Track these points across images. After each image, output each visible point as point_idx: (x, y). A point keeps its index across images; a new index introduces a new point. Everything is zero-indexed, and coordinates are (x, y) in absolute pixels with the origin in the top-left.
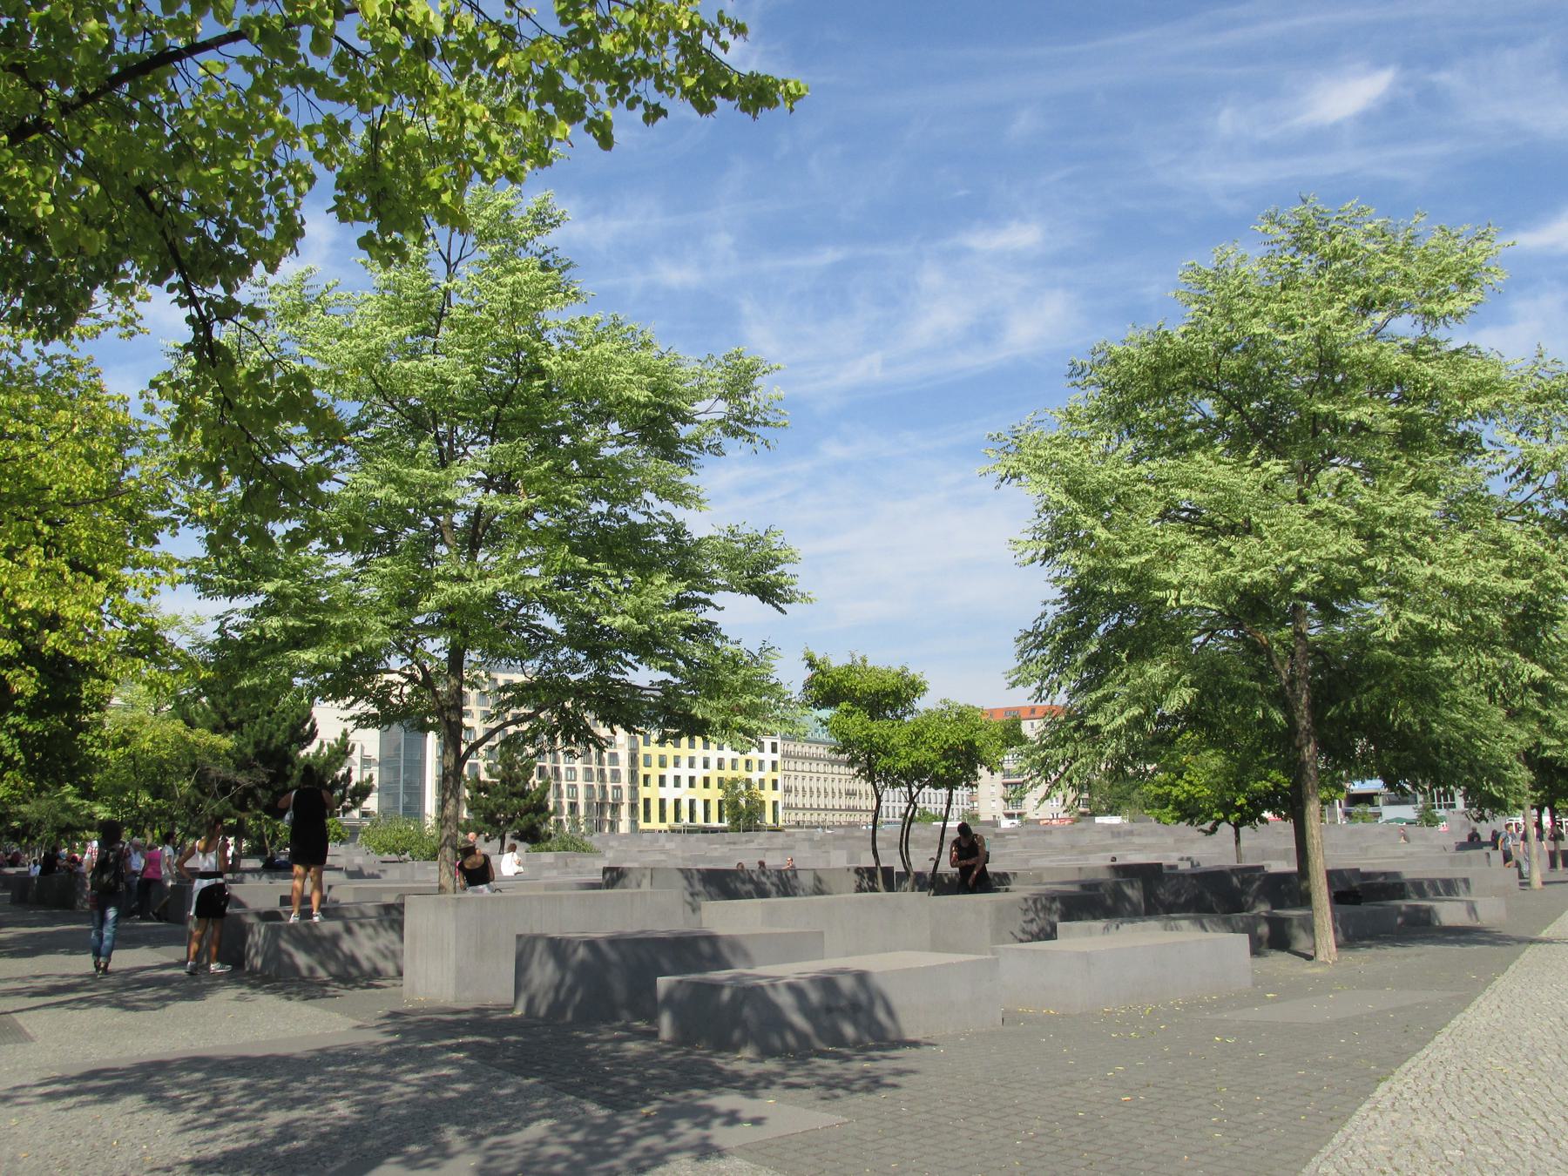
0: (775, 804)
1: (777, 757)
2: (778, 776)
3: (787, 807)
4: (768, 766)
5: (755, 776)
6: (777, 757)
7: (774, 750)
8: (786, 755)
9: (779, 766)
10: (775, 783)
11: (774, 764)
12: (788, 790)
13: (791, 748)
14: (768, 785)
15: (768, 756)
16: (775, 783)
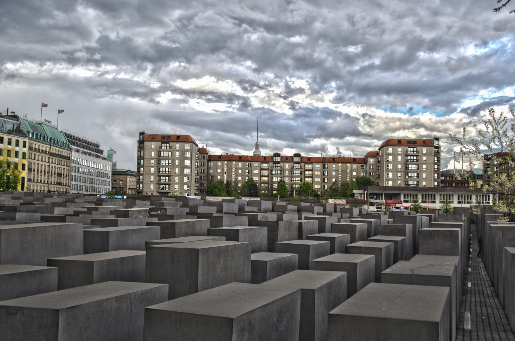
0: (23, 178)
1: (26, 150)
2: (26, 162)
3: (29, 180)
4: (20, 155)
5: (13, 159)
6: (26, 150)
7: (24, 146)
8: (30, 148)
9: (27, 157)
10: (24, 165)
11: (24, 154)
12: (30, 170)
13: (34, 146)
14: (20, 168)
15: (21, 150)
16: (24, 165)
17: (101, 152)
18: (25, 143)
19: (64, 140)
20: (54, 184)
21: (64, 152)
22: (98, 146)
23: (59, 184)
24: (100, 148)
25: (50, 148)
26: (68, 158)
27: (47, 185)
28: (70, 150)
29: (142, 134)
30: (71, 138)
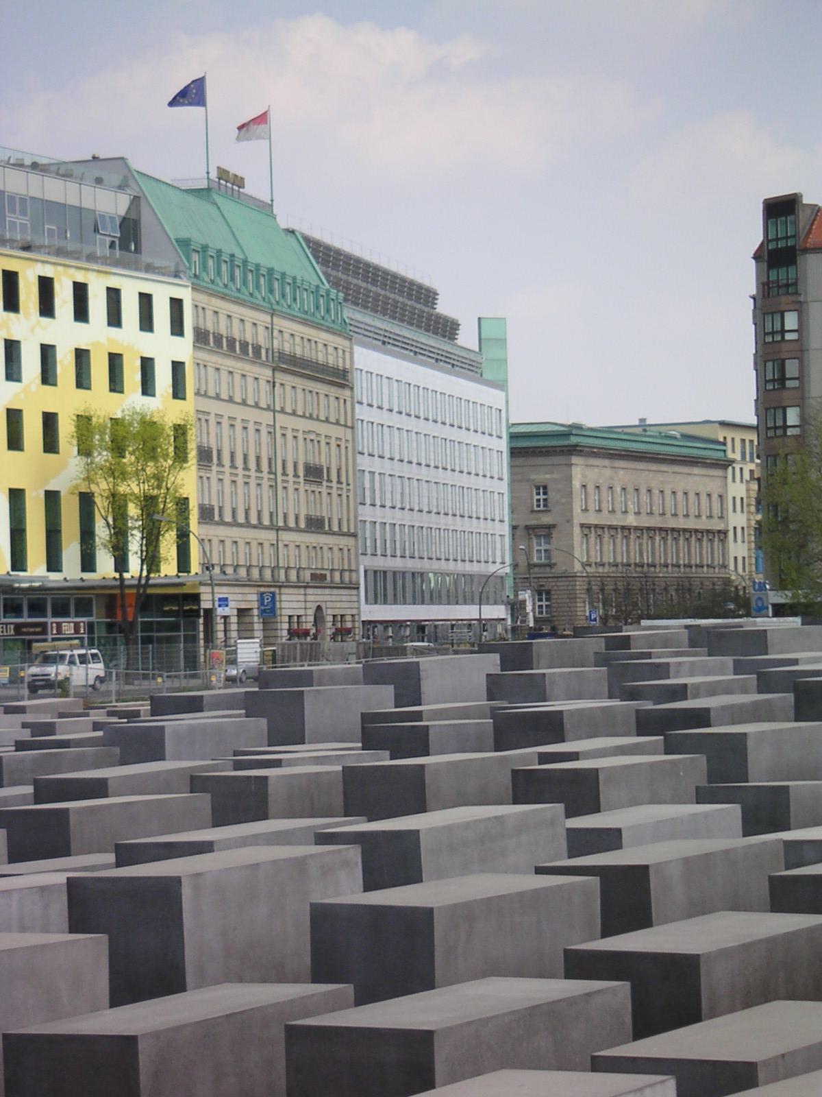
8: (201, 337)
12: (205, 456)
17: (448, 329)
18: (176, 304)
19: (309, 272)
20: (297, 529)
21: (323, 346)
22: (427, 296)
23: (316, 524)
24: (444, 307)
25: (270, 329)
26: (339, 378)
27: (271, 535)
28: (345, 331)
29: (780, 209)
30: (336, 266)
